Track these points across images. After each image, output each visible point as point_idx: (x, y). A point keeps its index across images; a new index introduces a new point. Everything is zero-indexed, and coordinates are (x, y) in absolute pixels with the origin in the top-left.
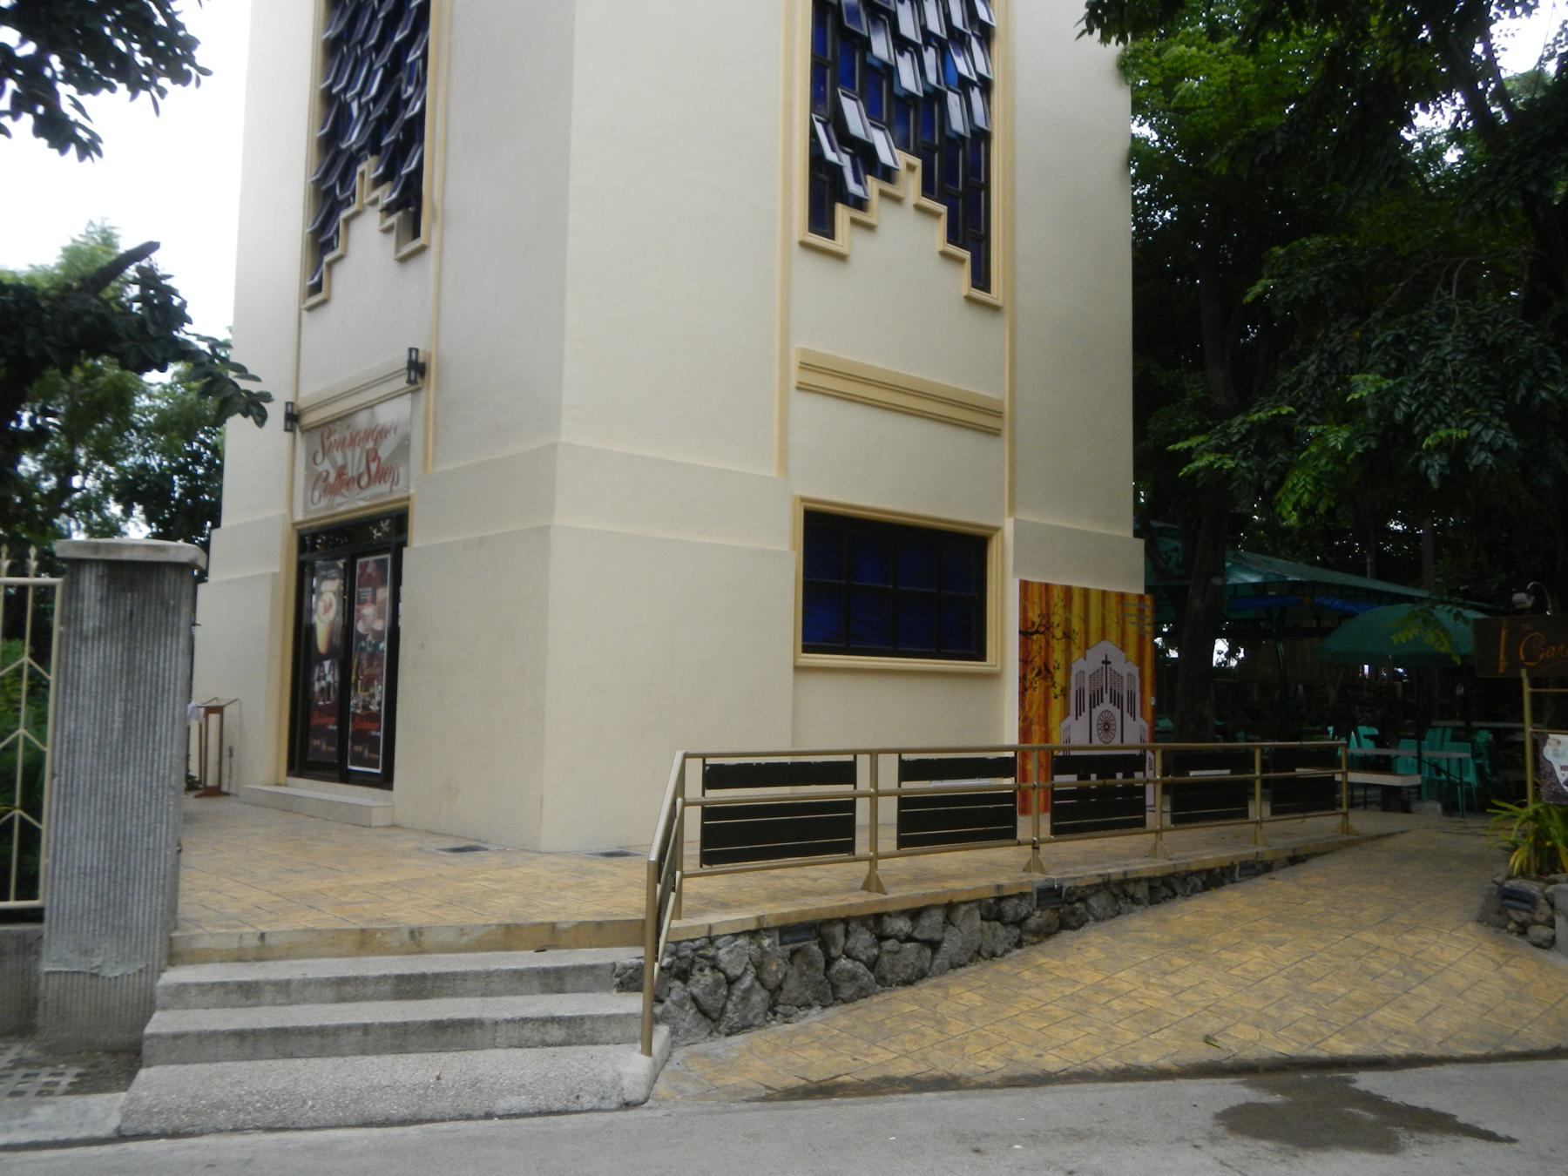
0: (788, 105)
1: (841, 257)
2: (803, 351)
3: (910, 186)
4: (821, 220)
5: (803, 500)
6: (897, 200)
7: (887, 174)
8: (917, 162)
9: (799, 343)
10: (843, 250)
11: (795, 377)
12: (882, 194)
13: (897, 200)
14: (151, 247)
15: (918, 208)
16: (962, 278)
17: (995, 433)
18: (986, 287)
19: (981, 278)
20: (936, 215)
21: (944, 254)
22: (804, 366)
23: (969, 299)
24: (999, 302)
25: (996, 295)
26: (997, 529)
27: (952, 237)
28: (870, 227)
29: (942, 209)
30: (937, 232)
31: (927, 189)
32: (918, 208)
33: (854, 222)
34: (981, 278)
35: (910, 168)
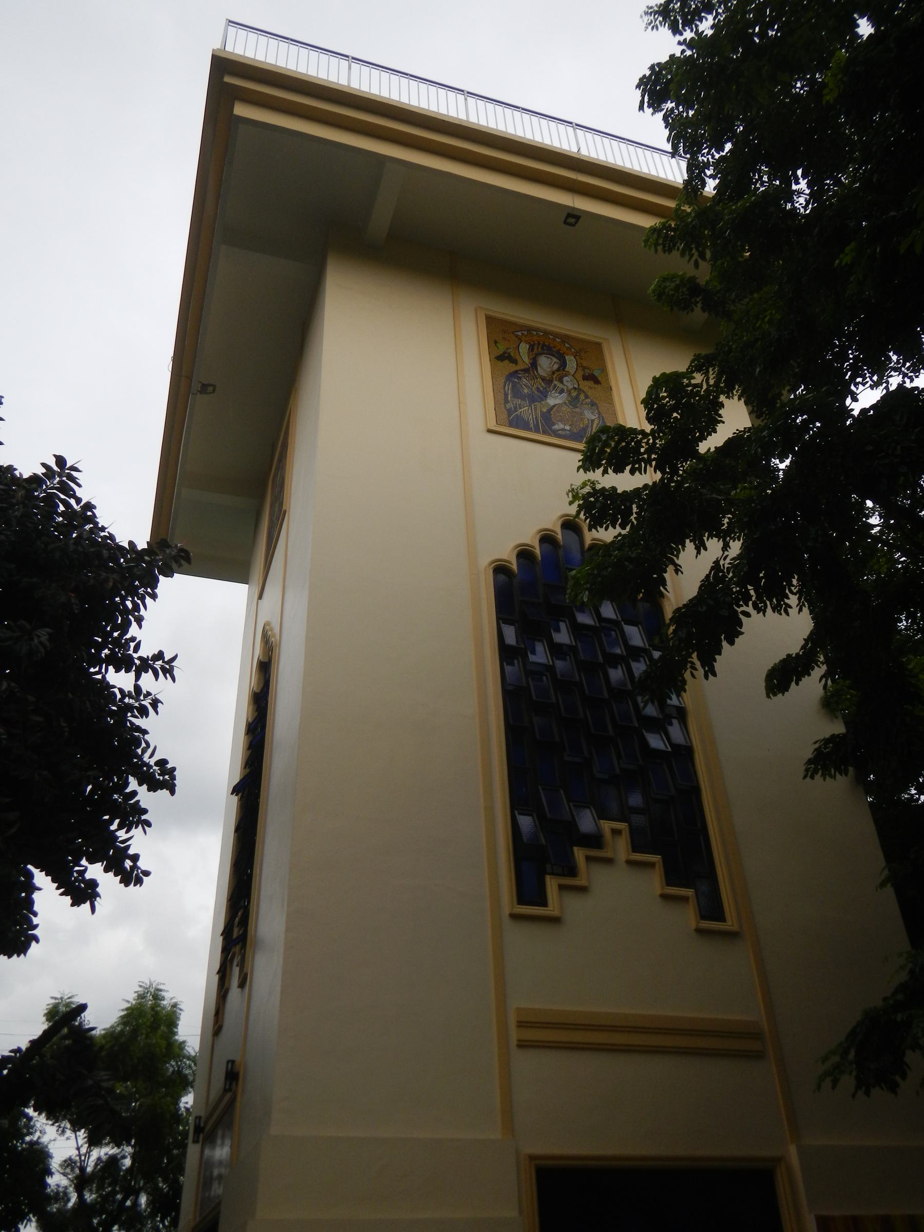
0: (490, 810)
1: (555, 920)
2: (518, 1010)
3: (621, 848)
4: (529, 891)
5: (532, 1158)
7: (594, 841)
10: (556, 913)
11: (514, 1035)
12: (589, 859)
13: (609, 861)
14: (83, 1008)
15: (630, 863)
16: (688, 917)
17: (758, 1056)
18: (721, 918)
19: (712, 909)
20: (652, 865)
21: (664, 897)
22: (521, 1024)
23: (700, 931)
24: (735, 928)
25: (731, 923)
26: (779, 1160)
27: (670, 880)
28: (583, 889)
29: (656, 858)
30: (653, 882)
31: (635, 848)
32: (630, 863)
33: (561, 887)
34: (712, 909)
35: (616, 832)
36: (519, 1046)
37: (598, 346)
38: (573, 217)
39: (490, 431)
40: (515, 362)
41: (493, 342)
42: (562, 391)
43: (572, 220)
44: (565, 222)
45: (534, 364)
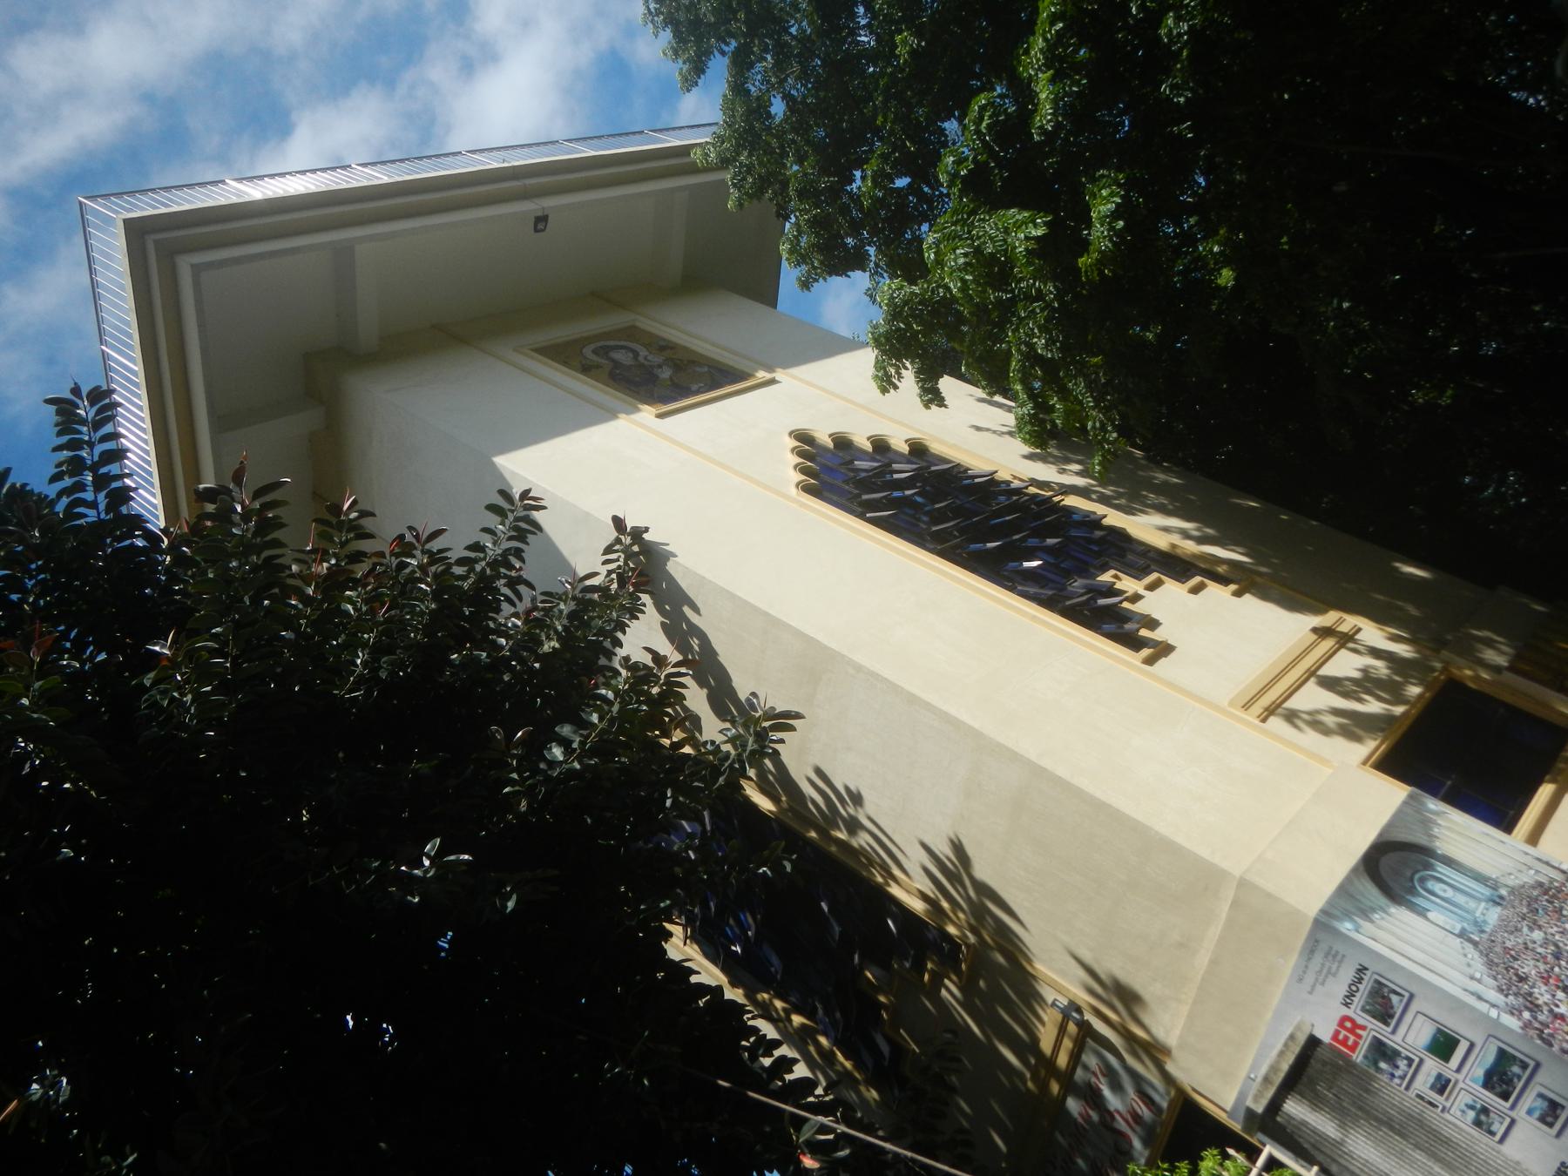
0: (1034, 618)
2: (1231, 704)
4: (1133, 642)
5: (1364, 763)
6: (1136, 598)
8: (1112, 572)
9: (1225, 703)
11: (1251, 717)
13: (1136, 598)
30: (1173, 590)
32: (1152, 587)
36: (1264, 721)
37: (634, 327)
38: (541, 221)
39: (660, 416)
40: (598, 367)
41: (566, 363)
42: (660, 366)
43: (540, 226)
44: (536, 230)
45: (613, 360)
